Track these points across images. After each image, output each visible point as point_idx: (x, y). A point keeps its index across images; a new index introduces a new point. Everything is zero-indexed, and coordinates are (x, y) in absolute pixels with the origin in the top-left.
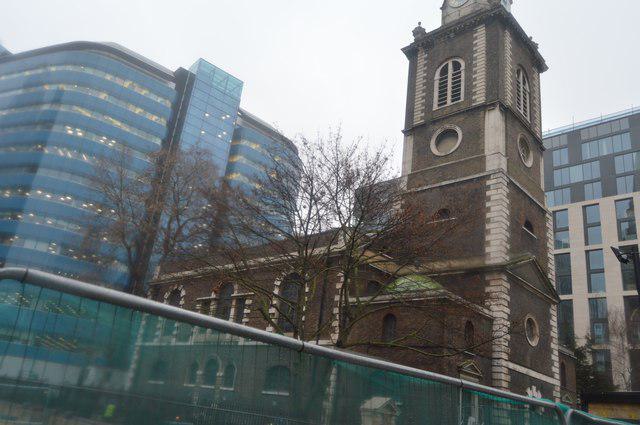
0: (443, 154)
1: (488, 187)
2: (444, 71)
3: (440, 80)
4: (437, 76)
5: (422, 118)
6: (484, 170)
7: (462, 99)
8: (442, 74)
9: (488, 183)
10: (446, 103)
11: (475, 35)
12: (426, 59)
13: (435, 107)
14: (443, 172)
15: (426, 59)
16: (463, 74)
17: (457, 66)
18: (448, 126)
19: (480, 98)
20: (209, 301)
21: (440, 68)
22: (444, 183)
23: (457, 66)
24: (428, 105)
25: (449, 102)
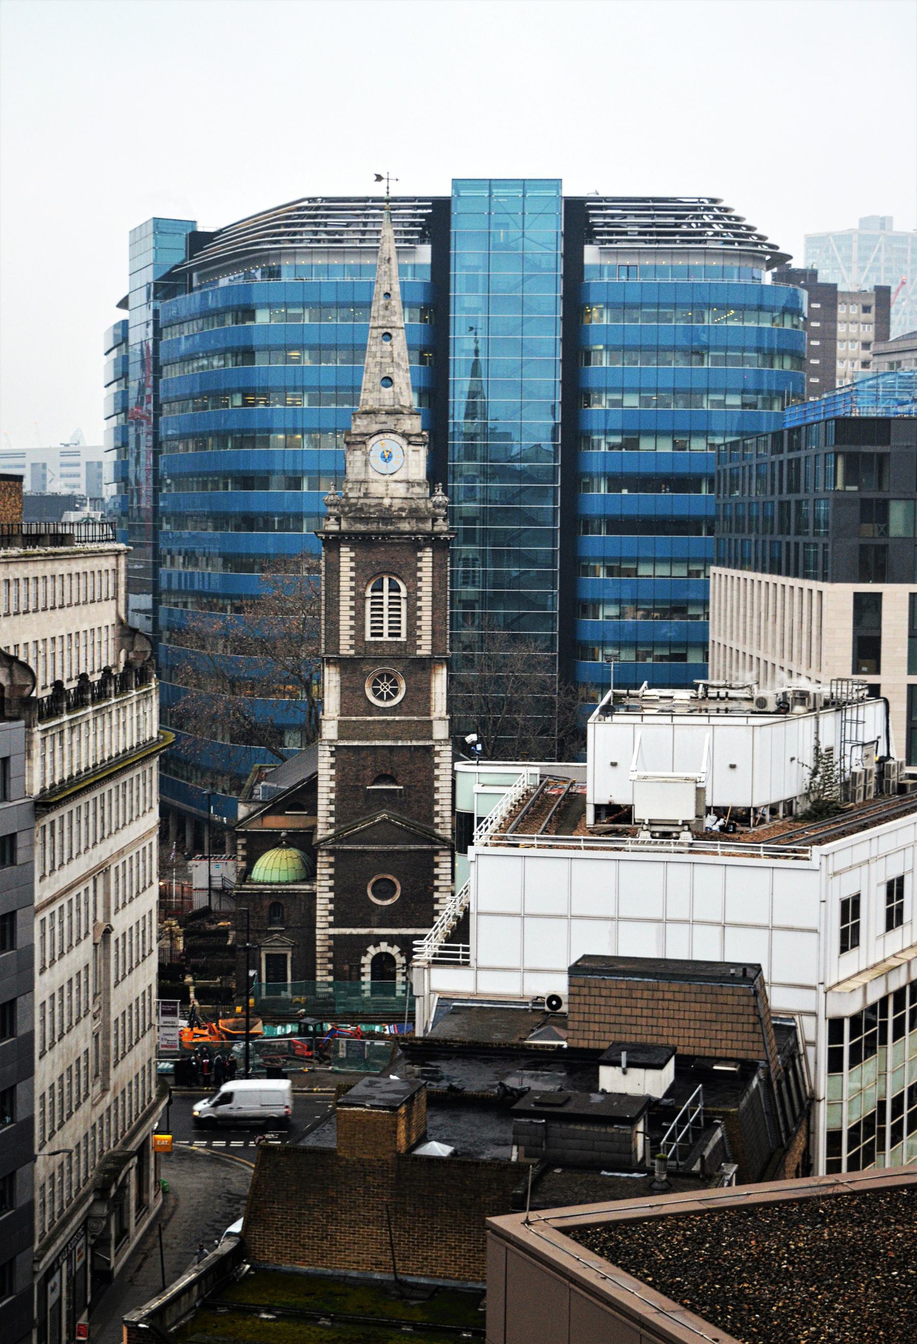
2: (379, 588)
3: (373, 597)
4: (369, 593)
5: (351, 647)
6: (430, 738)
7: (403, 638)
8: (373, 590)
10: (381, 635)
11: (419, 554)
12: (352, 559)
13: (368, 638)
14: (386, 730)
15: (352, 559)
17: (395, 588)
19: (425, 649)
23: (395, 588)
24: (359, 628)
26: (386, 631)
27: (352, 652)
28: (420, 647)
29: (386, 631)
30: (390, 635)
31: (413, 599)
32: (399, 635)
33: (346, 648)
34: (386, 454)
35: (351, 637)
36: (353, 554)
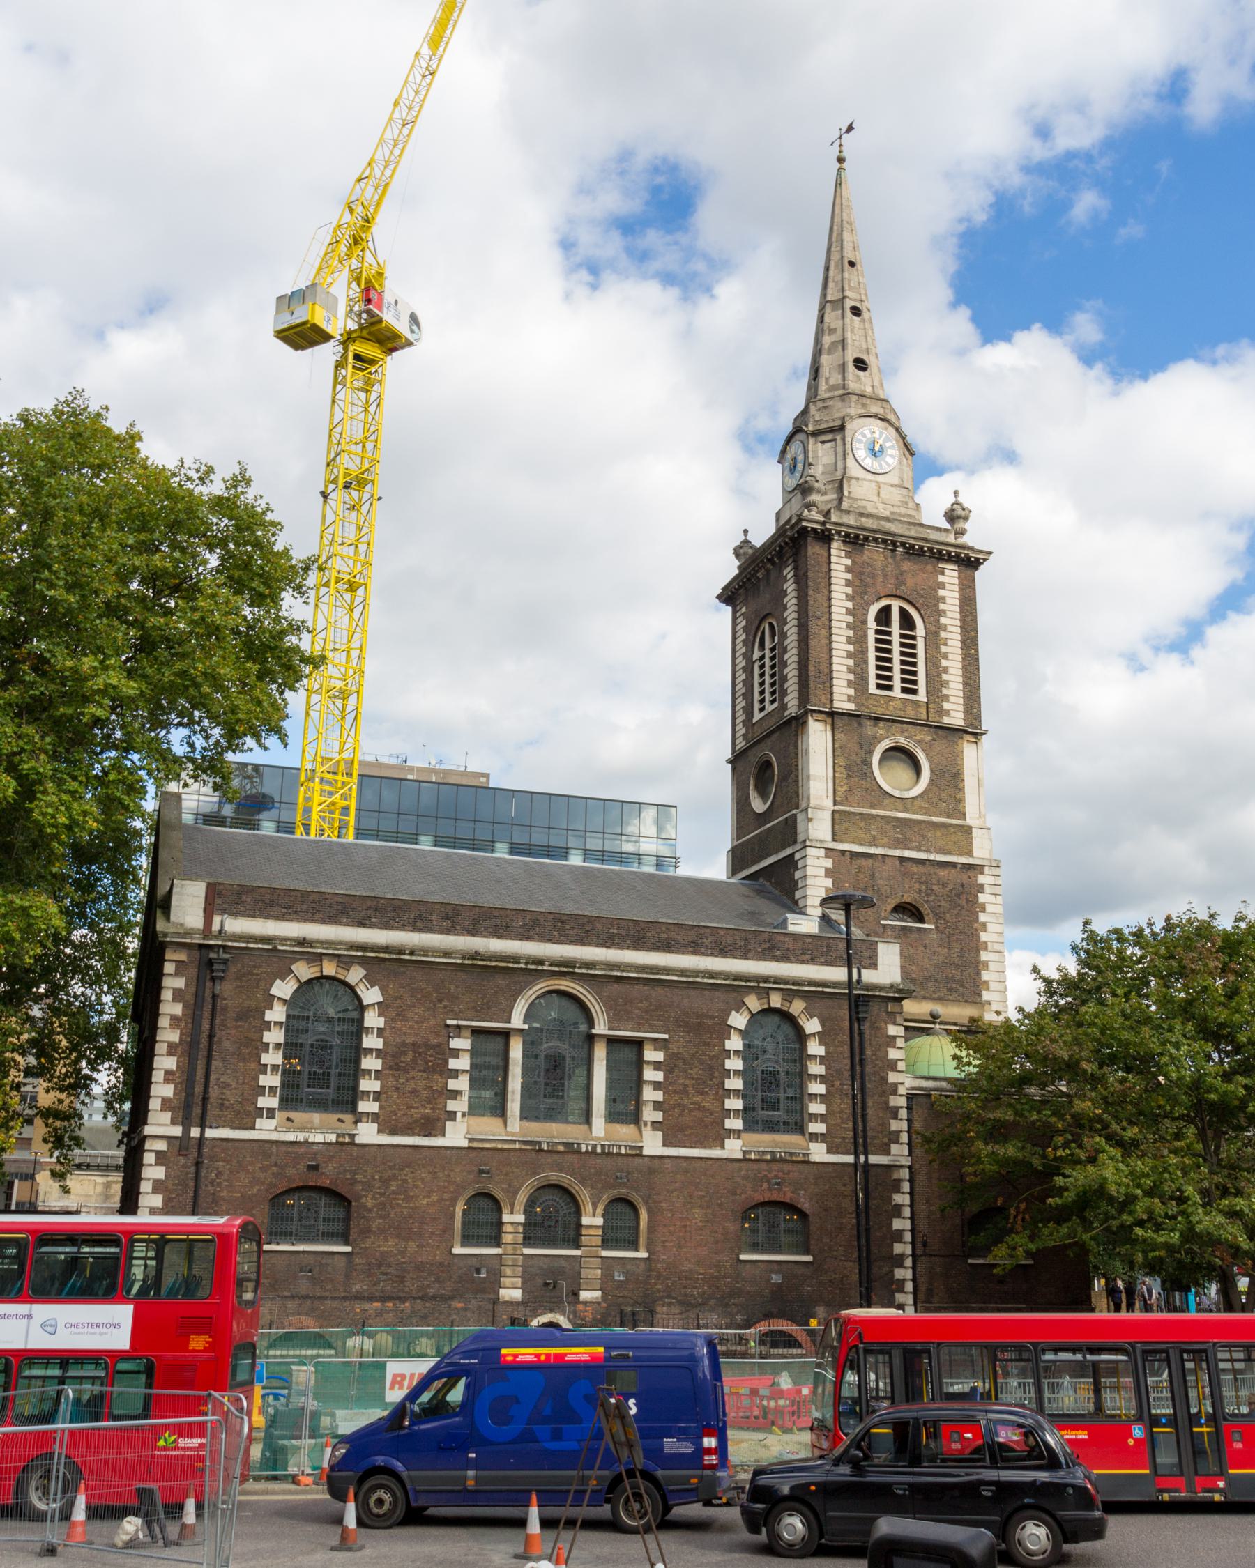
0: (897, 794)
1: (981, 888)
4: (872, 624)
6: (970, 853)
7: (922, 697)
9: (981, 879)
10: (890, 688)
13: (872, 689)
14: (905, 831)
15: (848, 570)
16: (920, 643)
18: (902, 741)
19: (956, 718)
20: (506, 1035)
21: (874, 610)
22: (908, 854)
25: (897, 692)
26: (897, 684)
27: (851, 707)
28: (947, 713)
29: (897, 684)
30: (904, 690)
31: (934, 639)
32: (914, 692)
33: (843, 698)
34: (877, 448)
35: (850, 683)
36: (849, 562)
